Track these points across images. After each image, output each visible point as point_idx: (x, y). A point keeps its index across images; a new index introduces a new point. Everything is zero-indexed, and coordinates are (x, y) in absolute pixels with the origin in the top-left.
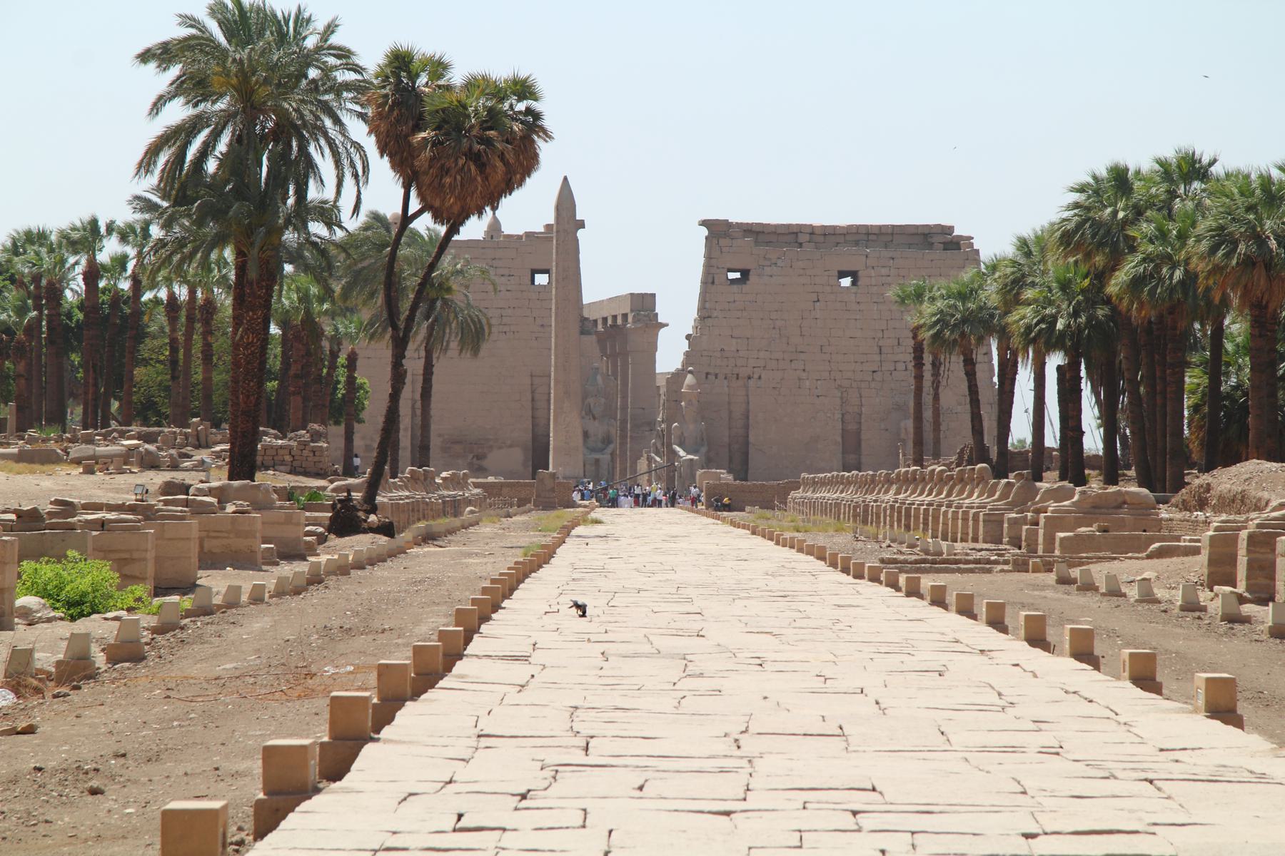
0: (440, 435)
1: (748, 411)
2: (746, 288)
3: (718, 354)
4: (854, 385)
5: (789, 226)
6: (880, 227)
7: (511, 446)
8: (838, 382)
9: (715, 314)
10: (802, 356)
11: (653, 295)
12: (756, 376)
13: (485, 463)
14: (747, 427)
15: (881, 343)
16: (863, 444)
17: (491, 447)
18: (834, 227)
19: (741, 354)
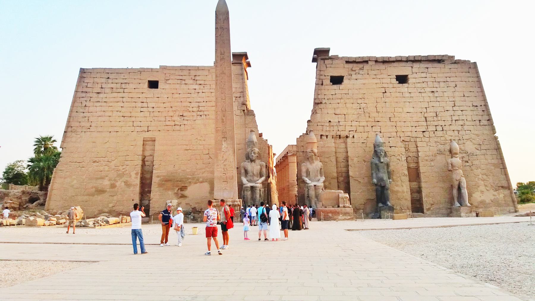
0: (158, 177)
1: (347, 157)
2: (341, 86)
3: (328, 124)
4: (412, 140)
5: (363, 57)
6: (415, 57)
7: (202, 182)
8: (402, 139)
9: (324, 102)
10: (379, 124)
12: (351, 136)
13: (186, 193)
14: (347, 166)
15: (426, 115)
16: (422, 176)
17: (190, 182)
18: (389, 58)
19: (341, 124)
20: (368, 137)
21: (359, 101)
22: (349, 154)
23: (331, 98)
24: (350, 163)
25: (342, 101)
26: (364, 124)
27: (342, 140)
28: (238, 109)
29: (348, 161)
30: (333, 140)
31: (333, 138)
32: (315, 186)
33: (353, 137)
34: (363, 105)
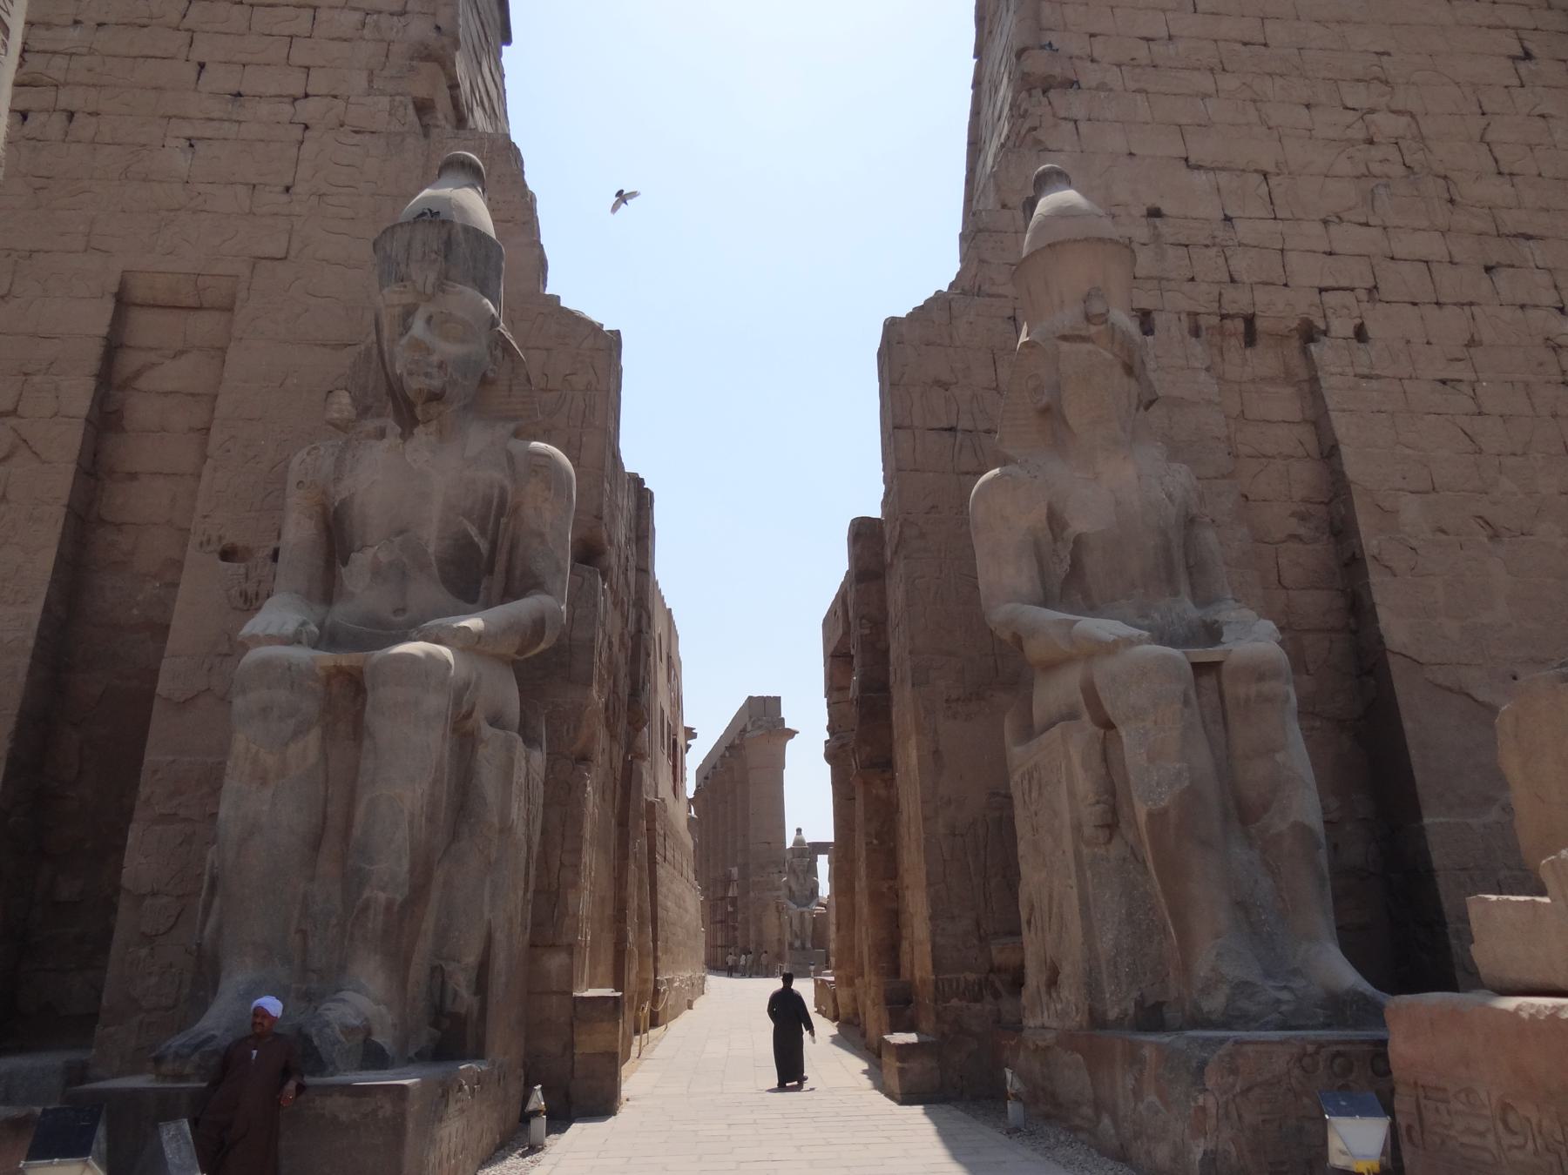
11: (778, 699)
12: (1342, 327)
19: (1243, 230)
20: (1472, 343)
21: (1358, 97)
22: (1353, 465)
23: (1142, 53)
24: (1371, 541)
25: (1229, 83)
26: (1430, 245)
27: (1264, 361)
28: (370, 91)
29: (1341, 530)
30: (1197, 347)
31: (1196, 332)
32: (1199, 668)
33: (1360, 334)
34: (1387, 125)
